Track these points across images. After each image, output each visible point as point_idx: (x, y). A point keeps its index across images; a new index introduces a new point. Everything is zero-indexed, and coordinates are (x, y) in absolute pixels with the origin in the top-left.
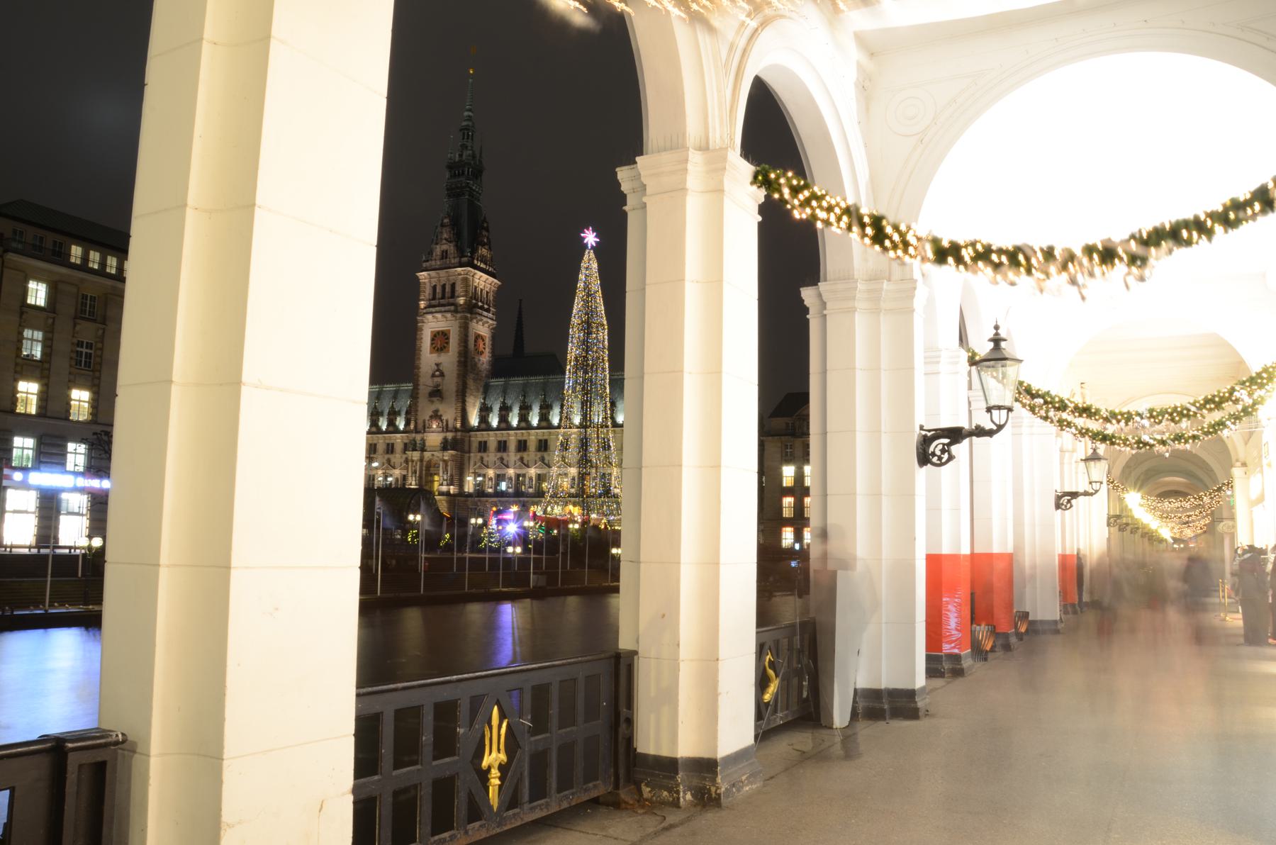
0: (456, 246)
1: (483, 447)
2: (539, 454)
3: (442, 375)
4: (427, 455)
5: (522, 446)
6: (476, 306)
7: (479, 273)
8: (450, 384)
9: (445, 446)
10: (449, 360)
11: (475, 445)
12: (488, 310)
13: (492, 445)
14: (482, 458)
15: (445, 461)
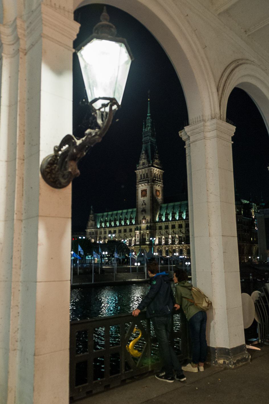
0: (147, 160)
1: (160, 228)
2: (179, 229)
3: (145, 204)
4: (142, 231)
5: (173, 227)
6: (155, 180)
7: (156, 169)
8: (148, 207)
9: (147, 228)
10: (147, 199)
11: (158, 228)
12: (160, 181)
13: (163, 227)
14: (160, 232)
15: (148, 234)
